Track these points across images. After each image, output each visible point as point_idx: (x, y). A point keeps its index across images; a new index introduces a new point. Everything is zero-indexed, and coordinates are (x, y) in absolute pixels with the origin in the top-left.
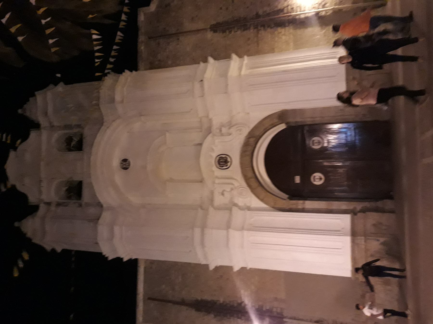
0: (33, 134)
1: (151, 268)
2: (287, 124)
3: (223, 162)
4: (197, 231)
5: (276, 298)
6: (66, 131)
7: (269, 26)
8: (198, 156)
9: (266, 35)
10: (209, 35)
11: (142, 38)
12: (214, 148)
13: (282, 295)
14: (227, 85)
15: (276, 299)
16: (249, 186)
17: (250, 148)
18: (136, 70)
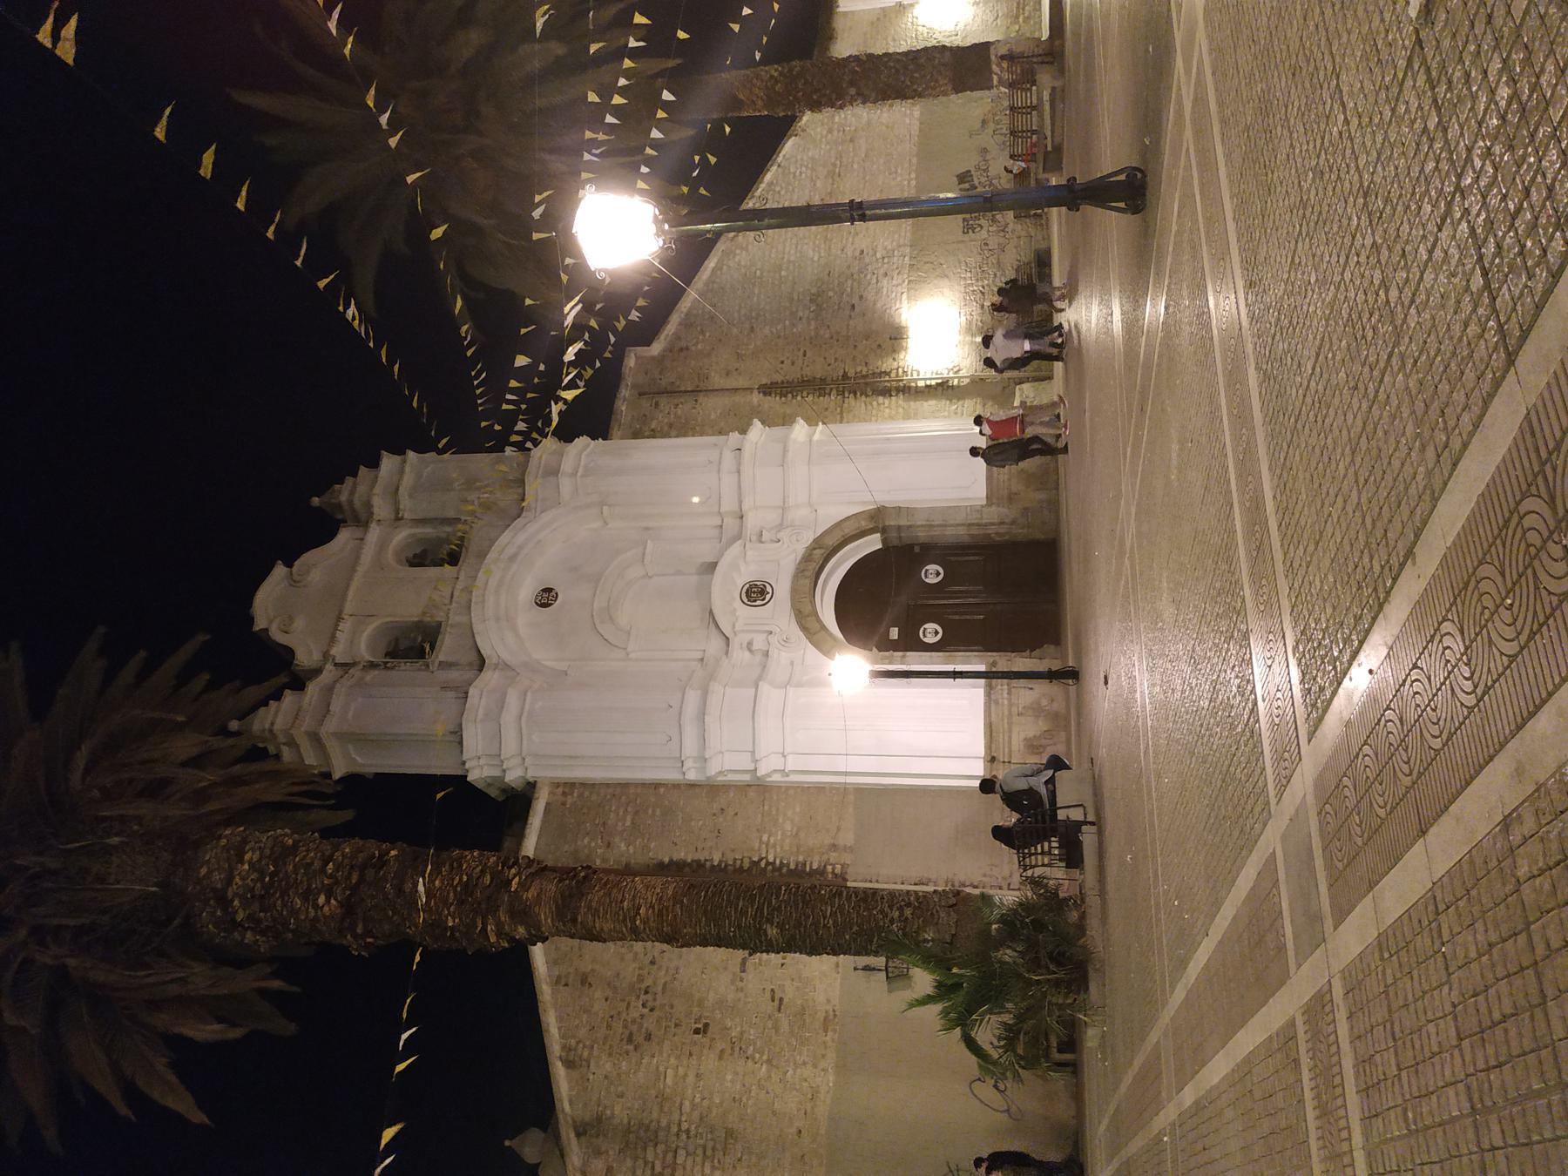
0: (344, 536)
1: (564, 804)
2: (884, 531)
3: (756, 593)
4: (693, 697)
5: (834, 845)
6: (428, 531)
7: (864, 393)
8: (704, 592)
9: (858, 405)
10: (756, 398)
11: (624, 392)
12: (743, 569)
13: (847, 838)
14: (785, 451)
15: (834, 847)
16: (804, 629)
17: (814, 566)
18: (605, 439)
